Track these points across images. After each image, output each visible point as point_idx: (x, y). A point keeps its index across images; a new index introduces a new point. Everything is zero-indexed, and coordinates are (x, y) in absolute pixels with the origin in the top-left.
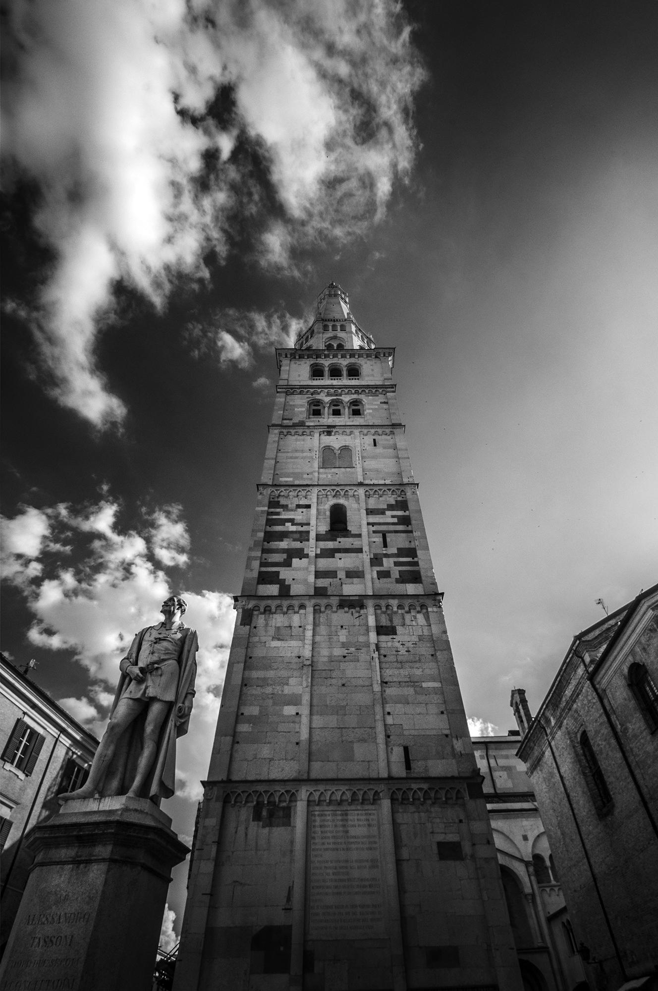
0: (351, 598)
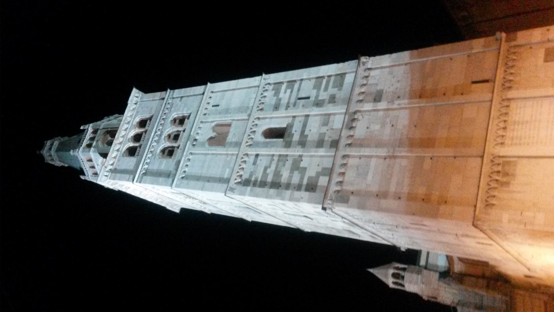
0: (346, 120)
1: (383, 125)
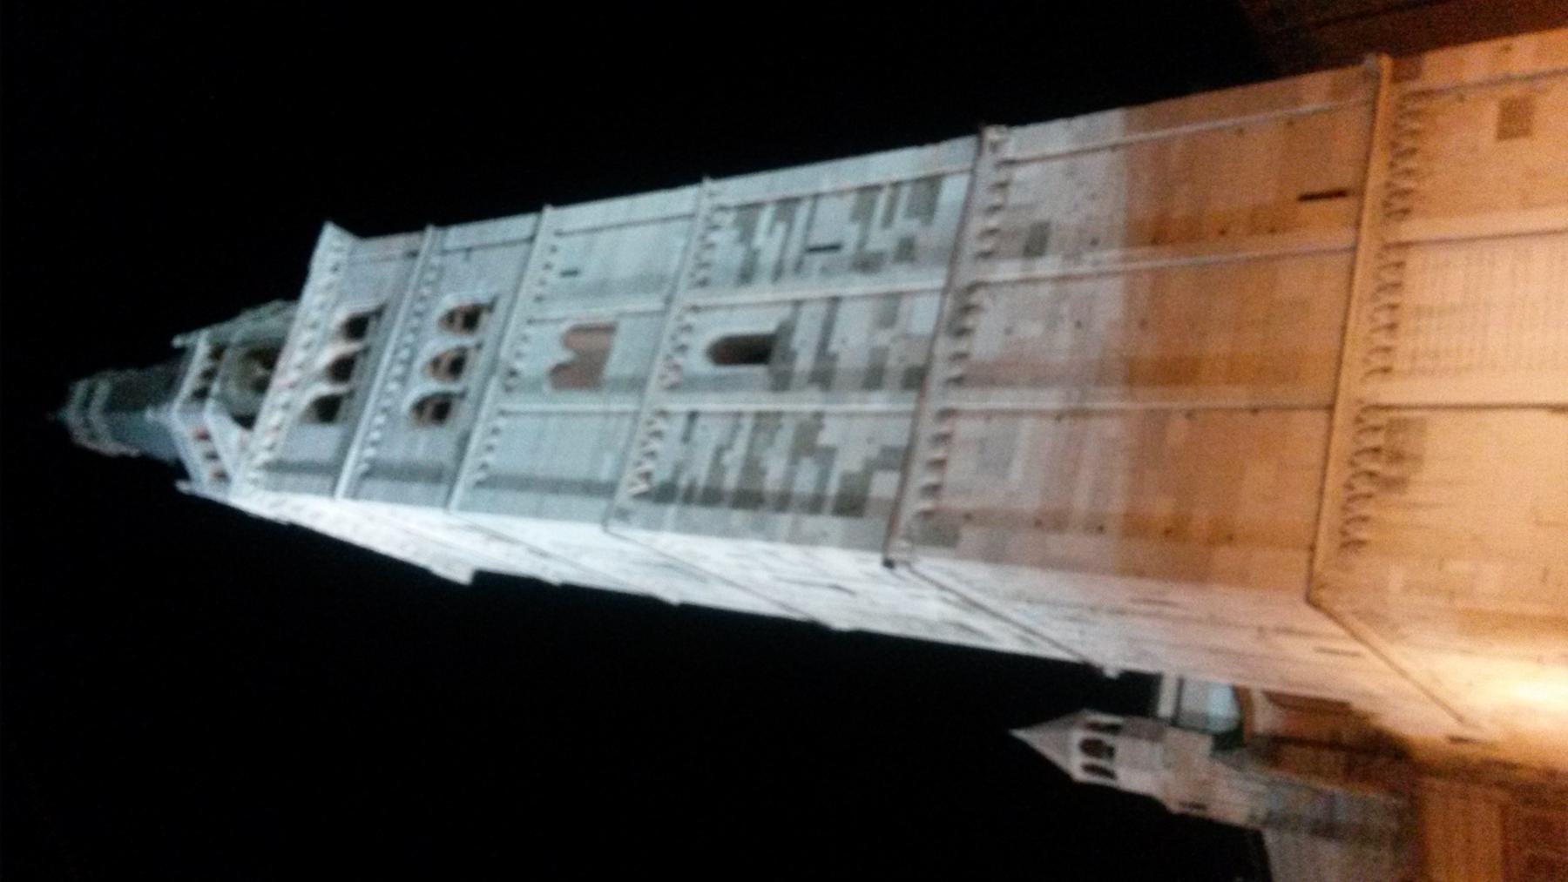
1: (1052, 322)
